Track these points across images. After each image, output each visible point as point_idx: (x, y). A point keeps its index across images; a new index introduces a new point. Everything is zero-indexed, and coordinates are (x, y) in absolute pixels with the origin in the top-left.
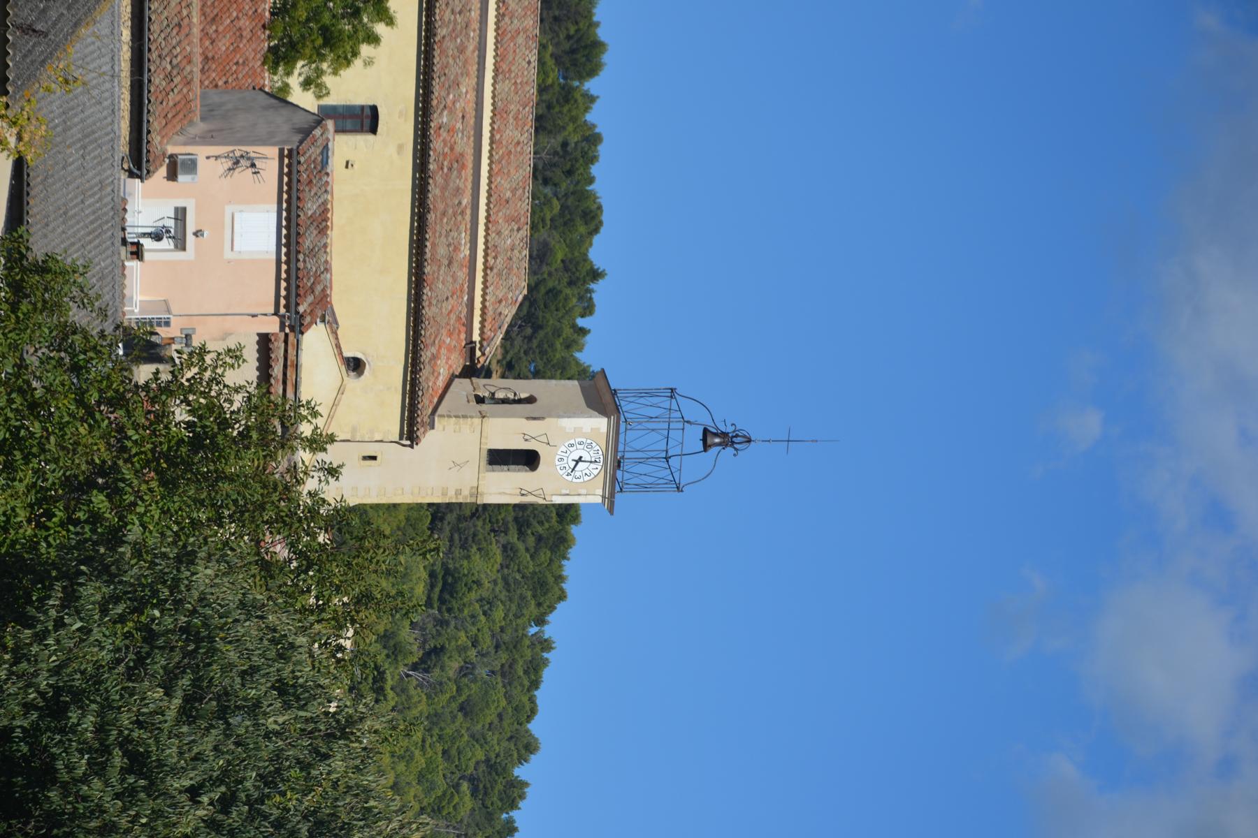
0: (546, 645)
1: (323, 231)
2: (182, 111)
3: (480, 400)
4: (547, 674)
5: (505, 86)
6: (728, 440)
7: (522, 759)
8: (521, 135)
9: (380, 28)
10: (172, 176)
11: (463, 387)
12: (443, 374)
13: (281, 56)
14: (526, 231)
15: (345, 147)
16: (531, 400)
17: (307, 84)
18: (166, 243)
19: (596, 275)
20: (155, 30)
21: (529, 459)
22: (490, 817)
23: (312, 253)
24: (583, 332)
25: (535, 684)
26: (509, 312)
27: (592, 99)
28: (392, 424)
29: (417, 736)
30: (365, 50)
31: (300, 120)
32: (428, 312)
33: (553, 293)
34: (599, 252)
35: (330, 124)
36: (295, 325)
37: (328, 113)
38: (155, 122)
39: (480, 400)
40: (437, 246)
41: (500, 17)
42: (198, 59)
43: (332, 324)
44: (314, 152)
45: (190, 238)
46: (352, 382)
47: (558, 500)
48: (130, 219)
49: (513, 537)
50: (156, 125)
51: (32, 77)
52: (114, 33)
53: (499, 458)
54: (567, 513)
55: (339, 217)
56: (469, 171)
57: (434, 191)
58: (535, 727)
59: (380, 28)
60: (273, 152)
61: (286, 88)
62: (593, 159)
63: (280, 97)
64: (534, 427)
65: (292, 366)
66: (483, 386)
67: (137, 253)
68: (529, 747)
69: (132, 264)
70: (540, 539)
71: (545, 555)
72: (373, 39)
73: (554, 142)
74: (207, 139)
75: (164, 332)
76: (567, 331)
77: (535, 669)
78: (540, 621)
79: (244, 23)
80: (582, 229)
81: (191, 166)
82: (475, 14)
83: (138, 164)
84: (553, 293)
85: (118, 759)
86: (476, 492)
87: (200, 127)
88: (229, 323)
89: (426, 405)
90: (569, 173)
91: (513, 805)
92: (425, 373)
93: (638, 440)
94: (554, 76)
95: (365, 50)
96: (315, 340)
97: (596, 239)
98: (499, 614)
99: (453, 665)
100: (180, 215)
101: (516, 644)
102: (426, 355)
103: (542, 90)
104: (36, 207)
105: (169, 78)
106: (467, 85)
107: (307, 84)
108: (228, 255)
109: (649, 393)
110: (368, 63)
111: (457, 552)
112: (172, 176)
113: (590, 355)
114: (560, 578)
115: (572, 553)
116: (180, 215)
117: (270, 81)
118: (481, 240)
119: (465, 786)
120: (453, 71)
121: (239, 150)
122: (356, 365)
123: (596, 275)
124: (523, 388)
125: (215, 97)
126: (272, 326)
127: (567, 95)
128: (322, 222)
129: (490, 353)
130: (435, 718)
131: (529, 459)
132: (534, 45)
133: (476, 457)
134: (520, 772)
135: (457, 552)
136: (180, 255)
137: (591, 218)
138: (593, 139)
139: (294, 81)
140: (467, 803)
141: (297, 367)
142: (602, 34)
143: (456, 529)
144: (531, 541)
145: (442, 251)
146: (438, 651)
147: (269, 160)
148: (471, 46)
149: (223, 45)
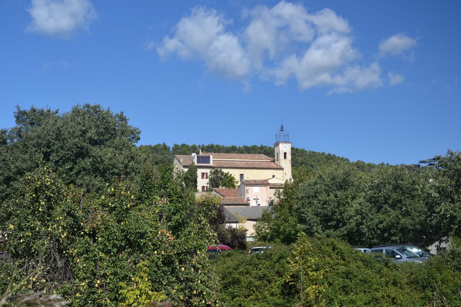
0: (310, 151)
1: (256, 181)
2: (241, 199)
3: (278, 160)
4: (314, 151)
5: (237, 158)
6: (282, 128)
7: (325, 154)
8: (243, 155)
9: (230, 174)
10: (249, 200)
11: (276, 162)
12: (274, 165)
13: (234, 187)
14: (256, 155)
15: (245, 178)
16: (277, 153)
17: (237, 183)
18: (258, 201)
19: (262, 146)
20: (230, 203)
21: (285, 153)
22: (333, 158)
23: (259, 182)
24: (269, 147)
25: (315, 152)
26: (266, 157)
27: (239, 147)
28: (281, 171)
29: (323, 167)
30: (232, 176)
31: (242, 184)
32: (266, 167)
33: (264, 151)
34: (259, 145)
35: (242, 180)
36: (268, 184)
37: (241, 181)
38: (242, 203)
39: (278, 160)
40: (258, 166)
41: (228, 159)
42: (234, 197)
43: (268, 179)
44: (246, 182)
45: (257, 198)
46: (276, 177)
47: (290, 150)
48: (255, 206)
49: (296, 156)
50: (243, 202)
51: (236, 218)
52: (231, 208)
53: (285, 157)
54: (292, 149)
55: (254, 179)
56: (248, 162)
57: (251, 167)
58: (321, 152)
59: (230, 174)
60: (246, 187)
61: (238, 186)
62: (247, 146)
63: (239, 187)
64: (281, 153)
65: (274, 184)
66: (276, 160)
67: (259, 205)
68: (323, 153)
69: (261, 205)
70: (296, 152)
71: (298, 151)
72: (231, 175)
73: (245, 151)
74: (244, 196)
75: (269, 201)
76: (269, 149)
77: (313, 152)
78: (307, 152)
79: (230, 191)
80: (256, 148)
81: (248, 198)
82: (228, 162)
83: (248, 205)
84: (264, 151)
85: (325, 206)
86: (290, 160)
87: (243, 197)
88: (268, 193)
89: (278, 167)
90: (249, 149)
91: (331, 155)
92: (274, 167)
93: (282, 140)
94: (236, 151)
95: (232, 176)
96: (270, 182)
97: (257, 146)
98: (306, 157)
99: (313, 163)
100: (254, 199)
101: (310, 155)
102: (272, 167)
103: (238, 153)
104: (253, 218)
105: (237, 201)
106: (237, 163)
107: (237, 183)
108: (259, 193)
109: (276, 138)
110: (234, 175)
111: (298, 163)
112: (249, 200)
113: (272, 146)
114: (301, 150)
115: (298, 148)
116: (254, 199)
117: (237, 188)
118: (230, 160)
119: (329, 161)
120: (235, 164)
121: (246, 192)
122: (273, 176)
123: (262, 146)
124: (276, 155)
125: (239, 195)
126: (268, 187)
127: (239, 150)
128: (255, 181)
129: (272, 159)
130: (320, 165)
131: (285, 153)
132: (232, 154)
133: (285, 160)
134: (327, 154)
135: (298, 163)
136: (259, 199)
137: (255, 146)
138: (244, 146)
139: (237, 185)
140: (331, 161)
141: (274, 184)
142: (231, 146)
143: (295, 163)
144: (296, 153)
145: (258, 165)
146: (311, 165)
147: (247, 188)
148: (232, 162)
149: (233, 194)
